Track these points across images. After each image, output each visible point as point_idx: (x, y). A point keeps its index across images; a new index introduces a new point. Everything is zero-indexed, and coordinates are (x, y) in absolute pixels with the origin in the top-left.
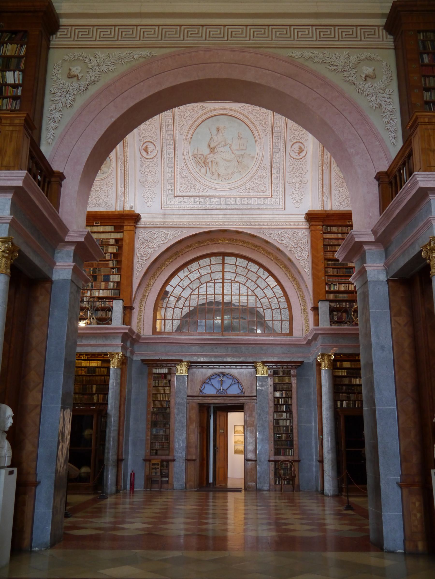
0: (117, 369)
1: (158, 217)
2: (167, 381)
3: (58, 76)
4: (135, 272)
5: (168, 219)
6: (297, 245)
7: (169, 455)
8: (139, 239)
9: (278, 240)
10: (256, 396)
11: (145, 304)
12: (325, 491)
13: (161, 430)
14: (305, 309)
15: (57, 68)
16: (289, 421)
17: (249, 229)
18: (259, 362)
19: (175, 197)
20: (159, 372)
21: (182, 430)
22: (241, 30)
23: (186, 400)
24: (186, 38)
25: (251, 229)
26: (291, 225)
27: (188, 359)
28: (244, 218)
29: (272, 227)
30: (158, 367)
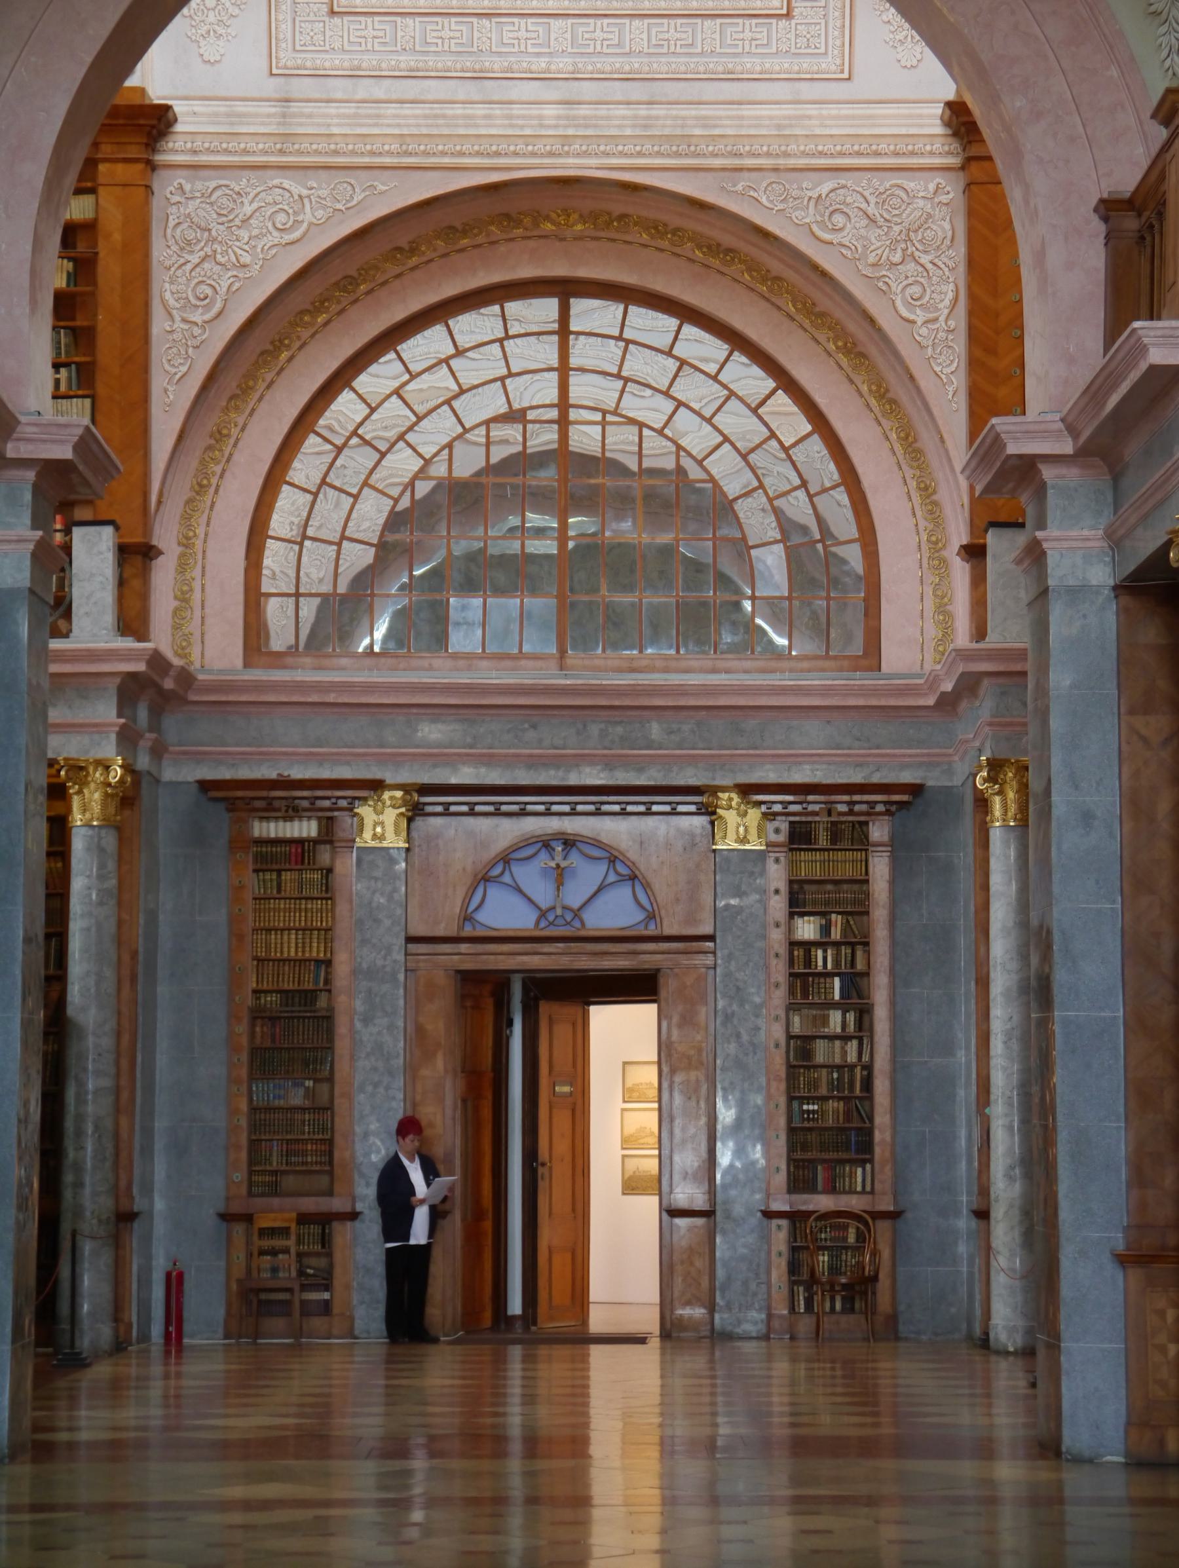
0: (103, 832)
1: (257, 115)
2: (317, 876)
4: (158, 382)
5: (301, 125)
6: (904, 250)
7: (330, 1193)
8: (171, 223)
9: (815, 228)
10: (711, 938)
11: (208, 525)
12: (992, 1336)
13: (295, 1085)
14: (937, 546)
16: (855, 1043)
17: (680, 174)
18: (724, 789)
19: (332, 13)
20: (281, 835)
21: (387, 1088)
23: (401, 957)
25: (691, 174)
26: (877, 154)
27: (407, 776)
28: (657, 118)
29: (792, 162)
30: (279, 810)
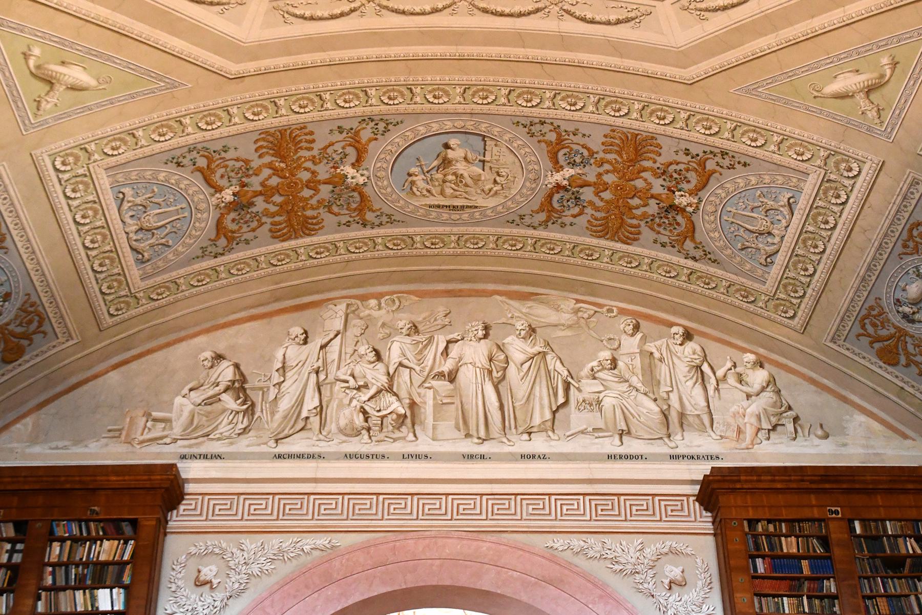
3: (179, 583)
15: (177, 568)
22: (472, 502)
24: (386, 517)
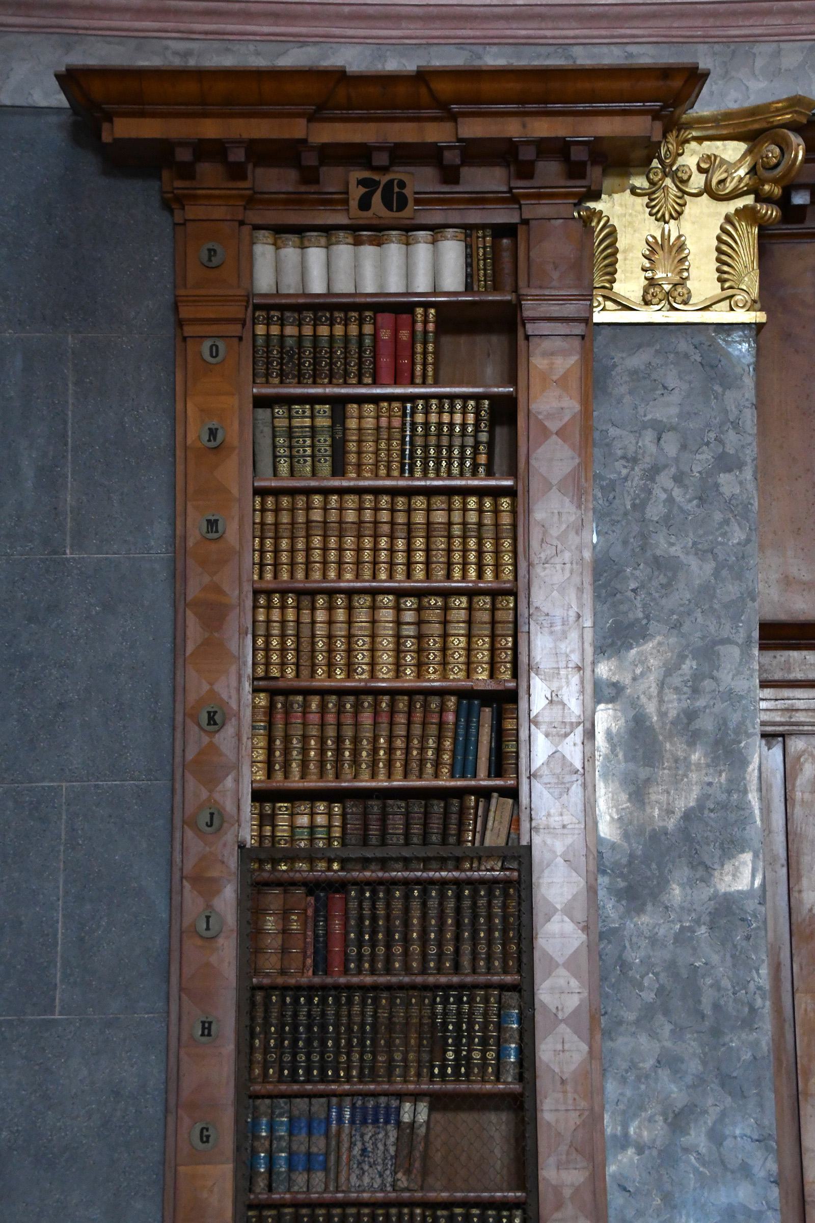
20: (344, 285)
